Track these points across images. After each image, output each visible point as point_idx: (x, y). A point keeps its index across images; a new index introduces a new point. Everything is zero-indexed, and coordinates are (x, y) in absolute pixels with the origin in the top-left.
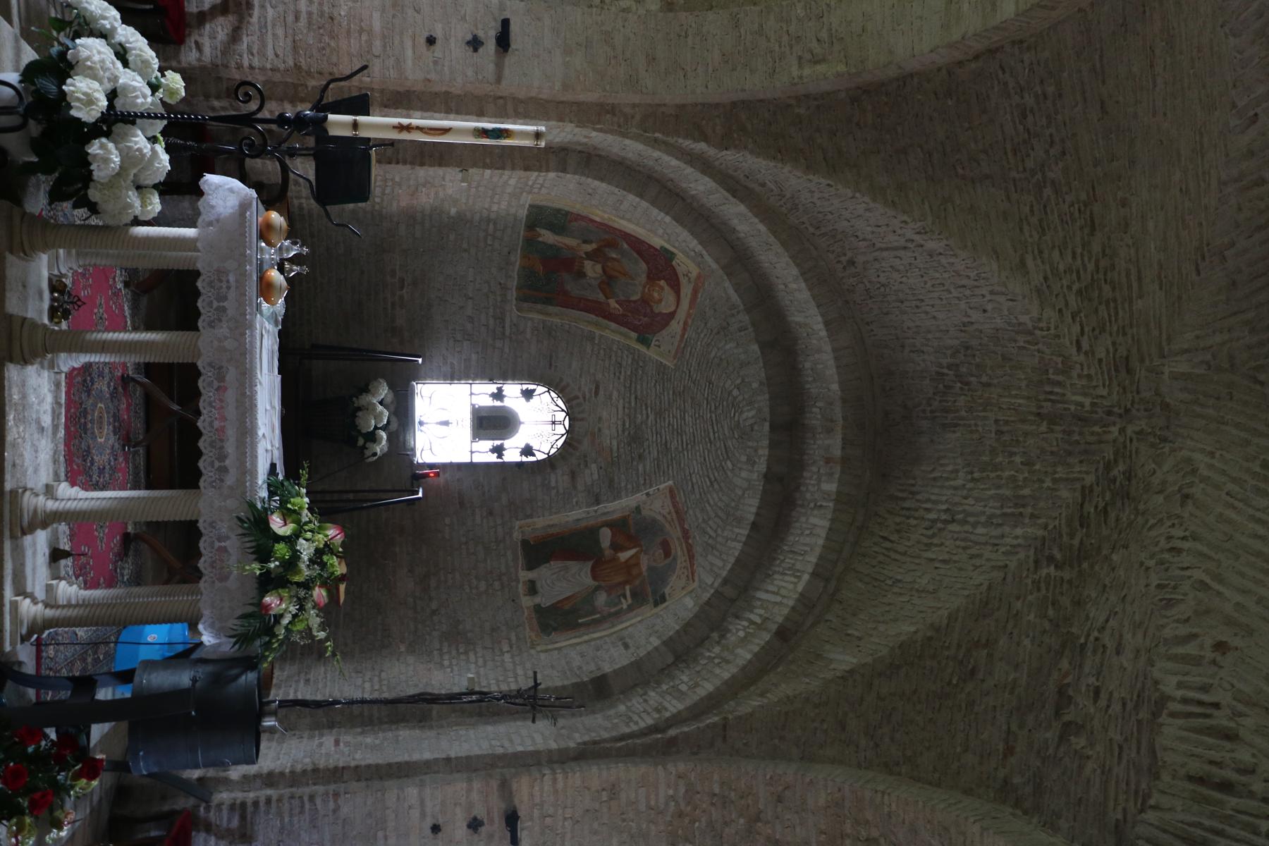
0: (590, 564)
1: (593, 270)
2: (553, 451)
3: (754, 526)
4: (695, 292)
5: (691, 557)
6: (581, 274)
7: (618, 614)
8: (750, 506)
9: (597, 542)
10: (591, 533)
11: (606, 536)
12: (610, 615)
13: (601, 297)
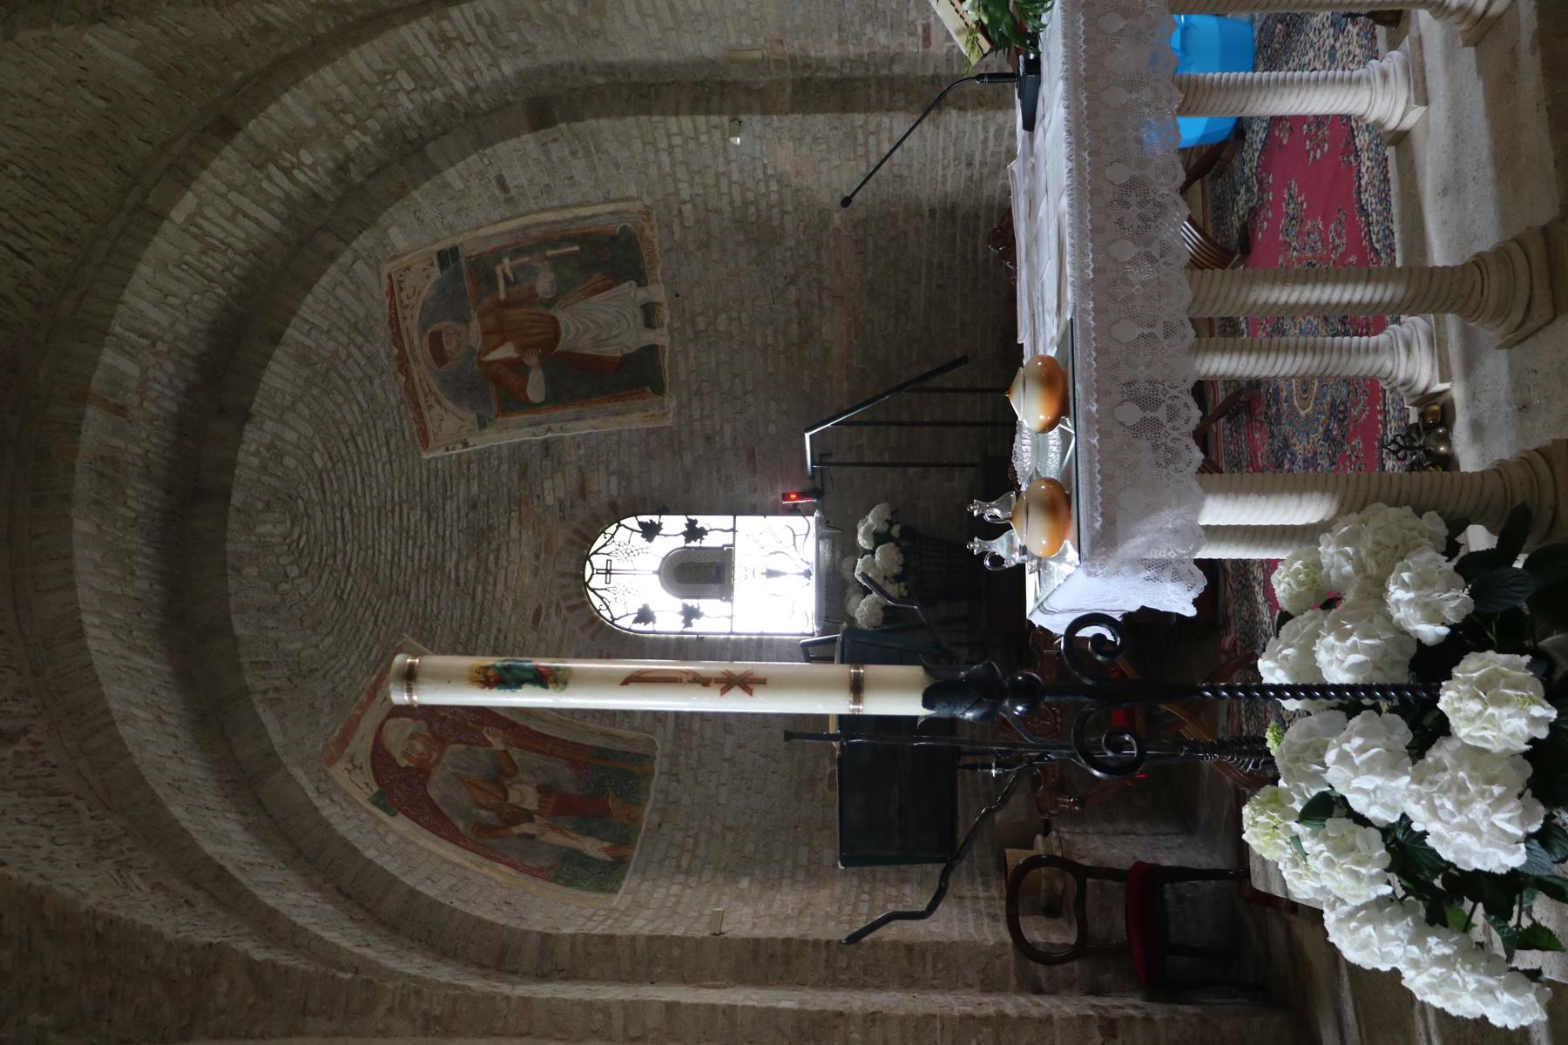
0: (559, 348)
1: (525, 795)
2: (612, 529)
3: (275, 339)
4: (344, 740)
5: (394, 322)
6: (544, 790)
7: (518, 251)
8: (279, 375)
9: (550, 381)
10: (558, 396)
11: (535, 388)
12: (527, 251)
13: (516, 754)
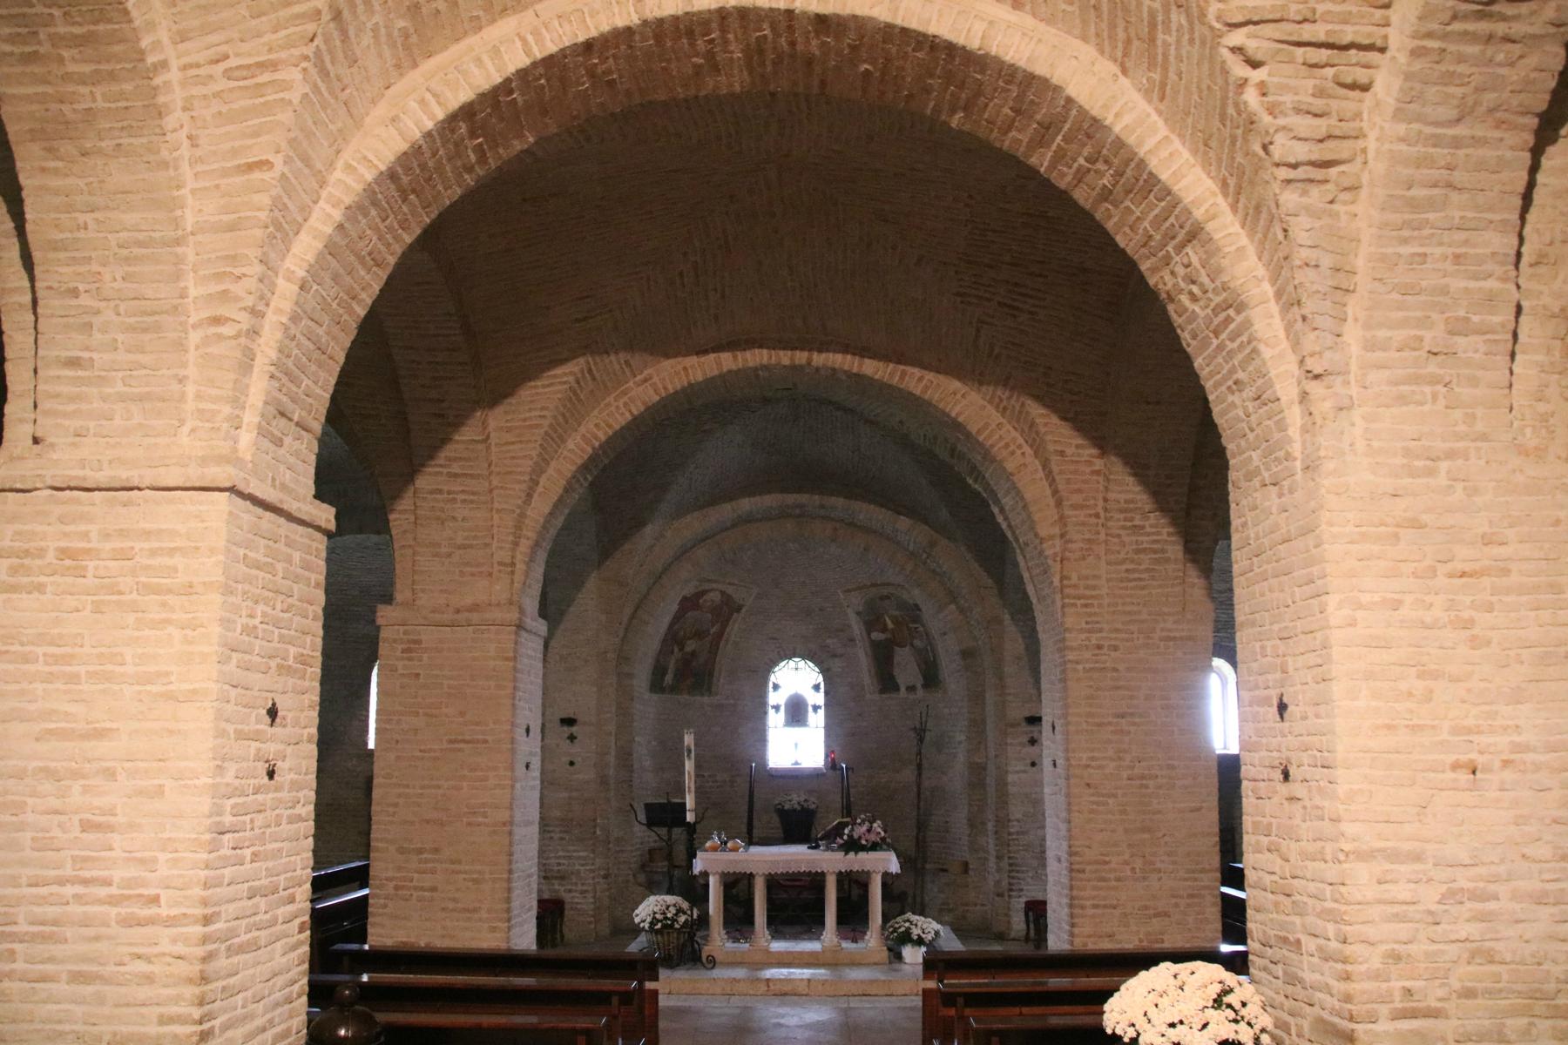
1: (691, 646)
5: (888, 584)
6: (693, 653)
10: (875, 645)
11: (875, 636)
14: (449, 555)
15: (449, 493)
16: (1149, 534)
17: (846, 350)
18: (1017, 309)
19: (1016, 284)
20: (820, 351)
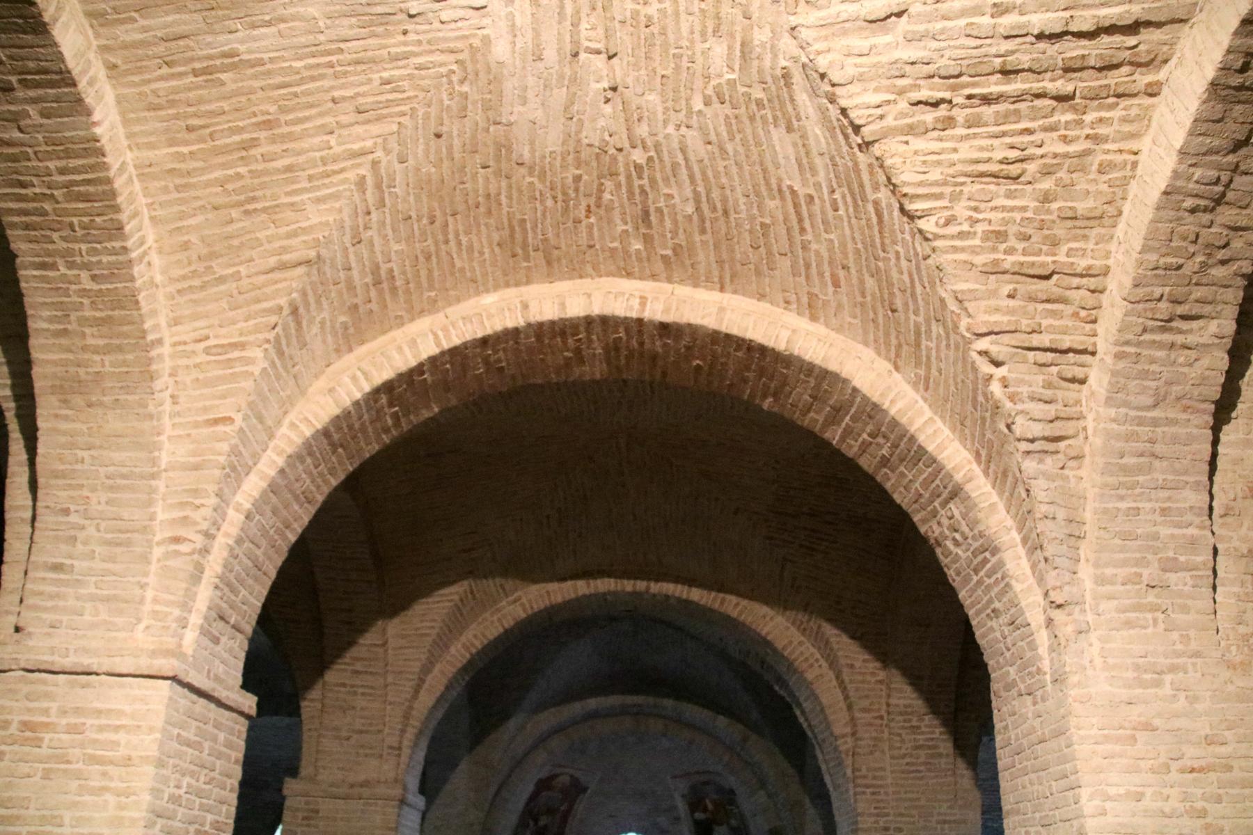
0: (716, 828)
5: (709, 772)
6: (546, 826)
10: (697, 823)
11: (699, 816)
14: (348, 739)
15: (352, 686)
16: (923, 733)
17: (677, 580)
18: (813, 549)
19: (813, 531)
20: (657, 581)
